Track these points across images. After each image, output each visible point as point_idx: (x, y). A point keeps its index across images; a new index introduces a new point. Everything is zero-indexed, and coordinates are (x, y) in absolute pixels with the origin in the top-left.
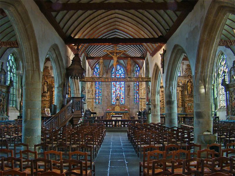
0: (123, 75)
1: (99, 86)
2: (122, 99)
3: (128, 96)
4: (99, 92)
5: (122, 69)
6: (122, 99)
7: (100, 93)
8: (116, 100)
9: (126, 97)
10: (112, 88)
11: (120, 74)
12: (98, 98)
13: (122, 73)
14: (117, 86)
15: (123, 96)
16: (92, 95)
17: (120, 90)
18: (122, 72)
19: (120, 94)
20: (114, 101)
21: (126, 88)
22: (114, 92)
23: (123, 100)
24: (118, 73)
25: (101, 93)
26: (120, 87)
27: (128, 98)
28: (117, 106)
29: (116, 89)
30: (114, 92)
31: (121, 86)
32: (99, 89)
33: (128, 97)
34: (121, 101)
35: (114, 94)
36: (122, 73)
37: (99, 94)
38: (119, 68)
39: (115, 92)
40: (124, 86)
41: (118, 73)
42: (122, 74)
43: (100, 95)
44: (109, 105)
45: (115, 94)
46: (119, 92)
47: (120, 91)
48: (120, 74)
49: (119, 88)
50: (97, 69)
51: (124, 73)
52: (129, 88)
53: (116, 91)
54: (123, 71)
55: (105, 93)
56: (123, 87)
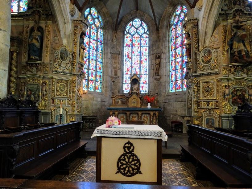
0: (147, 37)
1: (97, 55)
2: (144, 83)
3: (158, 77)
4: (96, 67)
5: (144, 25)
6: (144, 83)
7: (98, 70)
8: (131, 83)
9: (152, 80)
10: (125, 62)
11: (141, 36)
12: (94, 79)
13: (145, 33)
14: (133, 57)
15: (144, 78)
16: (73, 64)
17: (140, 65)
18: (145, 30)
19: (140, 74)
20: (126, 88)
21: (153, 62)
22: (128, 70)
23: (145, 85)
24: (137, 32)
25: (100, 69)
26: (140, 59)
27: (155, 81)
28: (134, 96)
29: (132, 63)
30: (128, 70)
31: (143, 59)
32: (96, 61)
33: (156, 79)
34: (142, 87)
35: (127, 74)
36: (145, 33)
37: (96, 71)
38: (140, 23)
39: (130, 69)
40: (147, 58)
41: (137, 32)
42: (145, 35)
43: (98, 74)
44: (117, 94)
45: (129, 73)
46: (138, 70)
47: (140, 68)
48: (141, 36)
49: (139, 62)
50: (93, 19)
51: (148, 33)
52: (157, 61)
53: (132, 67)
54: (146, 29)
55: (110, 70)
56: (146, 60)
